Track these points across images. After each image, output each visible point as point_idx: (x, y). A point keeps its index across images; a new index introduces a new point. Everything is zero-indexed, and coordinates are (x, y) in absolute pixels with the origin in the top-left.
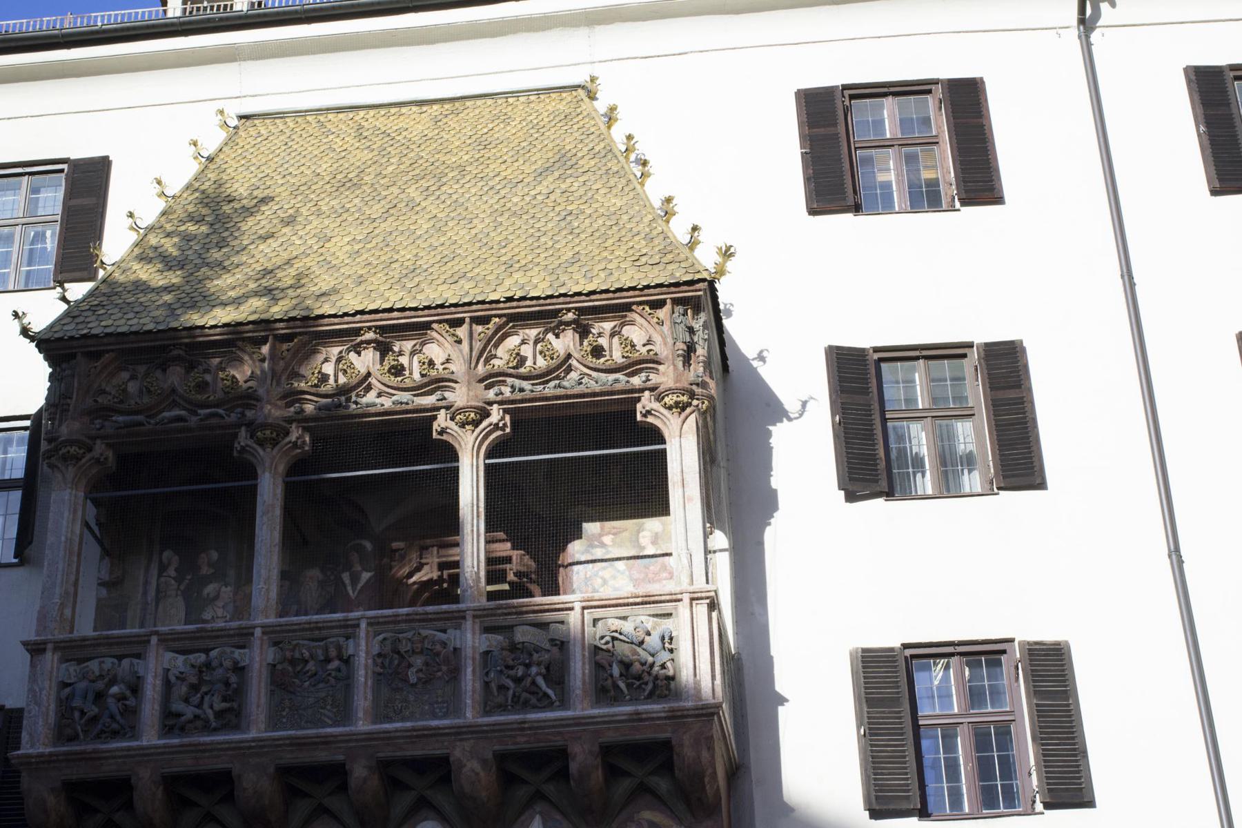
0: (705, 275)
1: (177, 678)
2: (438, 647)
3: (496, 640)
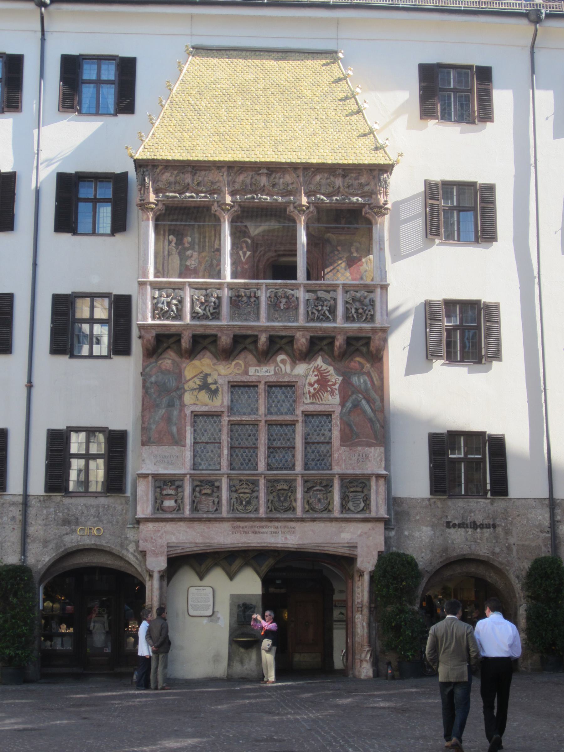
3: (311, 296)
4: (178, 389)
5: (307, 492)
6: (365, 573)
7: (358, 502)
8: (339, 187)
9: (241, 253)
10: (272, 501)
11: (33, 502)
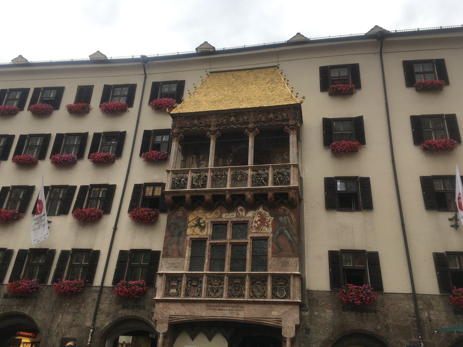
0: (299, 102)
1: (194, 178)
2: (244, 173)
4: (184, 226)
5: (251, 285)
6: (287, 339)
7: (282, 292)
8: (271, 118)
9: (227, 160)
10: (231, 290)
11: (105, 290)
